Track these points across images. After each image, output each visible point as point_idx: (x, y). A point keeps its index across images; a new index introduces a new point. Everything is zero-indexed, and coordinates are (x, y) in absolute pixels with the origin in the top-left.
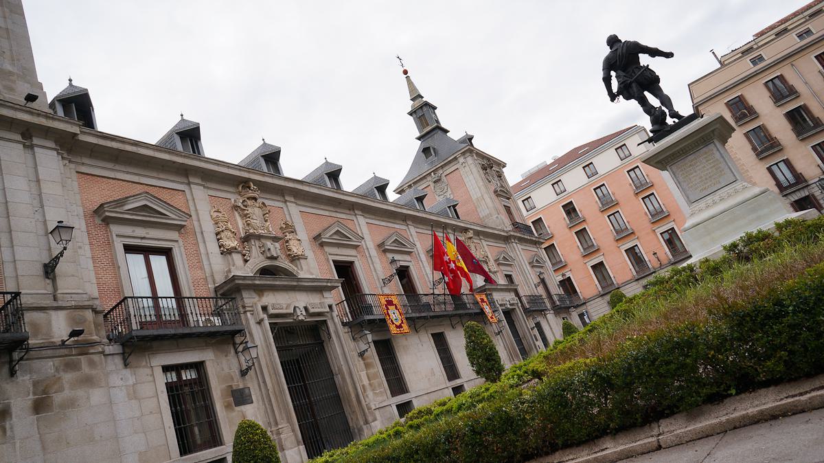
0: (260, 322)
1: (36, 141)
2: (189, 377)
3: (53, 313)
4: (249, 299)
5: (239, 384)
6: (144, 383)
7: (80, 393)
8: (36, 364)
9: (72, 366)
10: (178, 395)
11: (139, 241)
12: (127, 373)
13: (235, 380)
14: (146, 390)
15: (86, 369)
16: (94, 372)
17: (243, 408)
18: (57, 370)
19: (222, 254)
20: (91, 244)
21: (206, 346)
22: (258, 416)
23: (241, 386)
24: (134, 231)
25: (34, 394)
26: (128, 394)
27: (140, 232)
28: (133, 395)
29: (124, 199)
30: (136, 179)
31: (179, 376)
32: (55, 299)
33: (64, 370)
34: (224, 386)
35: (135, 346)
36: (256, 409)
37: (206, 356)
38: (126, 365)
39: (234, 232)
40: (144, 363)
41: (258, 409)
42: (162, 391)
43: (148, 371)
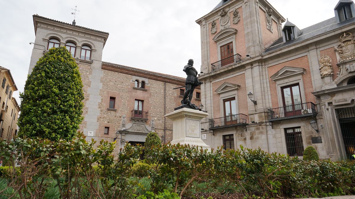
0: (328, 109)
1: (254, 65)
2: (289, 132)
3: (255, 115)
4: (325, 100)
5: (315, 135)
6: (278, 133)
7: (260, 136)
8: (251, 128)
9: (258, 129)
10: (292, 137)
11: (286, 84)
12: (273, 130)
13: (314, 133)
14: (278, 135)
15: (261, 130)
16: (263, 130)
17: (316, 144)
18: (255, 130)
19: (322, 78)
20: (271, 90)
21: (302, 121)
22: (324, 148)
23: (317, 136)
24: (284, 81)
25: (250, 135)
26: (273, 136)
27: (286, 80)
28: (275, 137)
29: (277, 72)
30: (286, 60)
31: (294, 131)
32: (256, 111)
33: (256, 130)
34: (308, 136)
35: (275, 123)
36: (324, 146)
37: (302, 124)
38: (273, 128)
39: (329, 66)
40: (278, 127)
41: (325, 145)
42: (283, 136)
43: (279, 130)
